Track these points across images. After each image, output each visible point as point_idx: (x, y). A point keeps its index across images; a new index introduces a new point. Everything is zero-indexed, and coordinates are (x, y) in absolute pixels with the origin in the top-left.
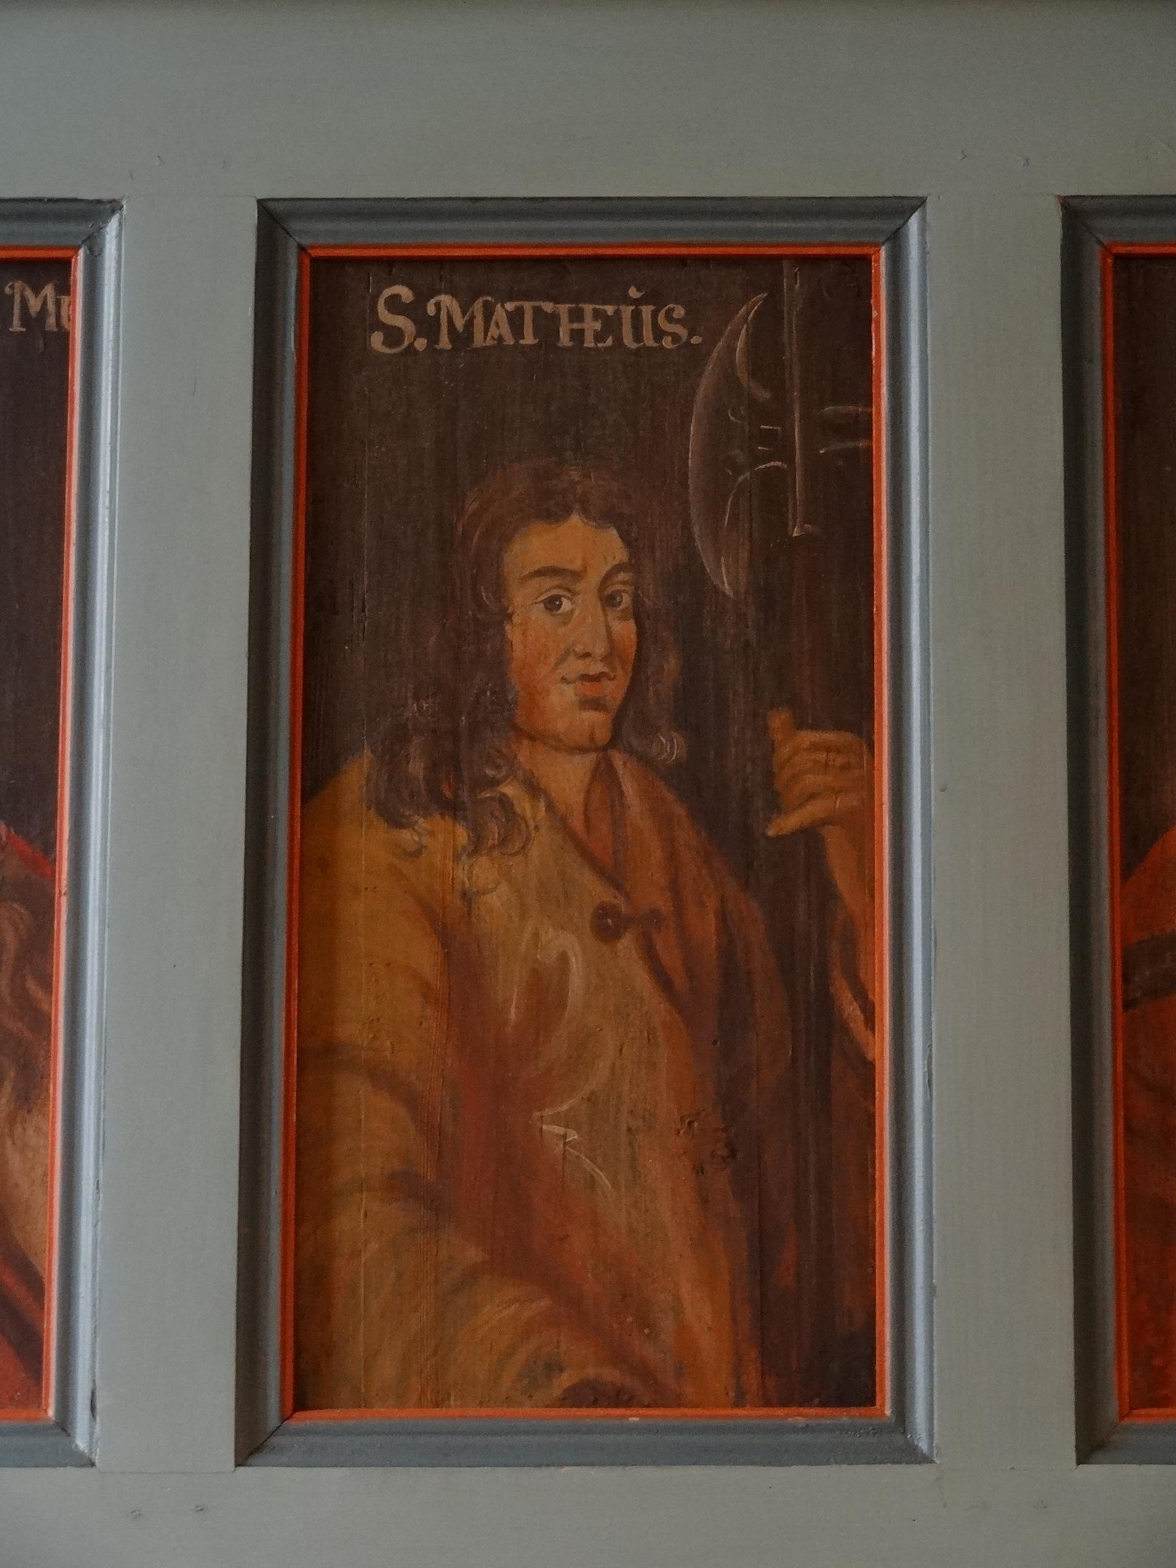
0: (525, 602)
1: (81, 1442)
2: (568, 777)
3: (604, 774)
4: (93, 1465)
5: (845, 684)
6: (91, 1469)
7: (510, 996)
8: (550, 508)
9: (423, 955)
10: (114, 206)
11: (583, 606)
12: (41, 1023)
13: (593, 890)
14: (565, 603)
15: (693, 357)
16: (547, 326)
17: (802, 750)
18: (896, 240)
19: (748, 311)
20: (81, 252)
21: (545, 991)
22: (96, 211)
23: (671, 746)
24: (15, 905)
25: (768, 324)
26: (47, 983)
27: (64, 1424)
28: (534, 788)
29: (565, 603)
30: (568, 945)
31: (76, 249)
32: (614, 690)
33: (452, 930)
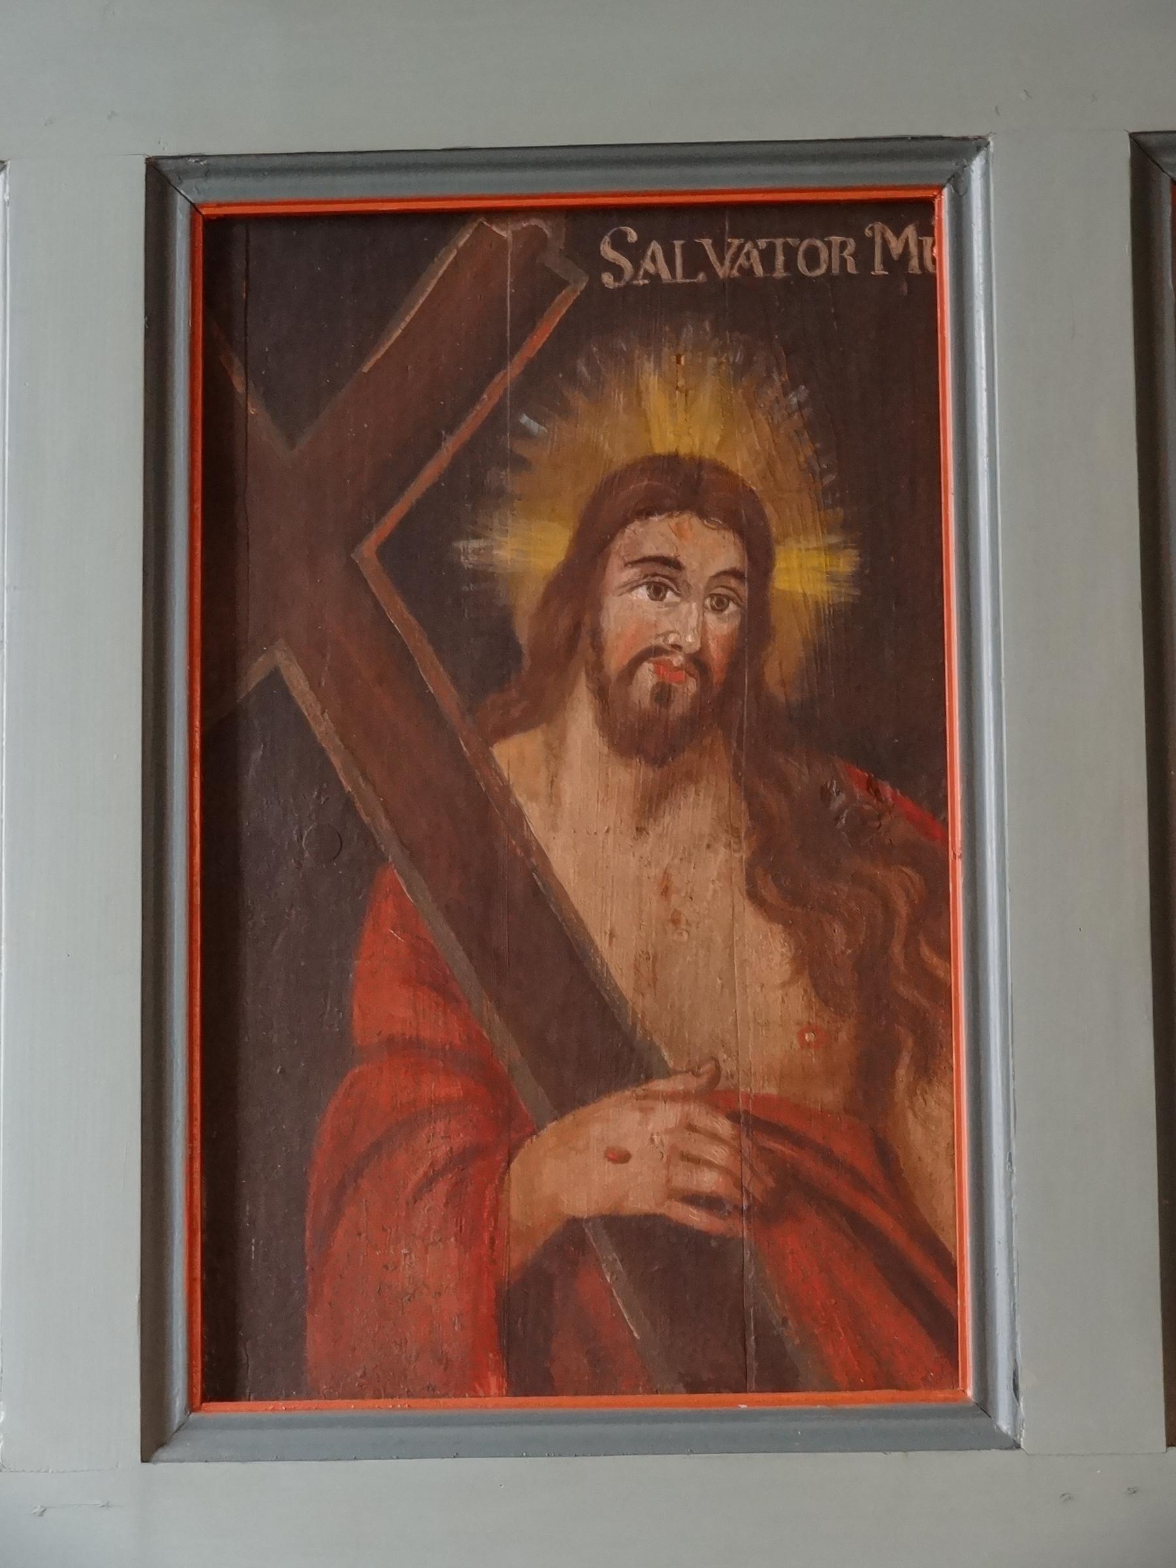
1: (1004, 1424)
4: (1018, 1447)
6: (1017, 1451)
10: (978, 144)
12: (941, 992)
20: (945, 191)
22: (964, 148)
24: (904, 869)
26: (945, 951)
27: (985, 1405)
31: (940, 188)
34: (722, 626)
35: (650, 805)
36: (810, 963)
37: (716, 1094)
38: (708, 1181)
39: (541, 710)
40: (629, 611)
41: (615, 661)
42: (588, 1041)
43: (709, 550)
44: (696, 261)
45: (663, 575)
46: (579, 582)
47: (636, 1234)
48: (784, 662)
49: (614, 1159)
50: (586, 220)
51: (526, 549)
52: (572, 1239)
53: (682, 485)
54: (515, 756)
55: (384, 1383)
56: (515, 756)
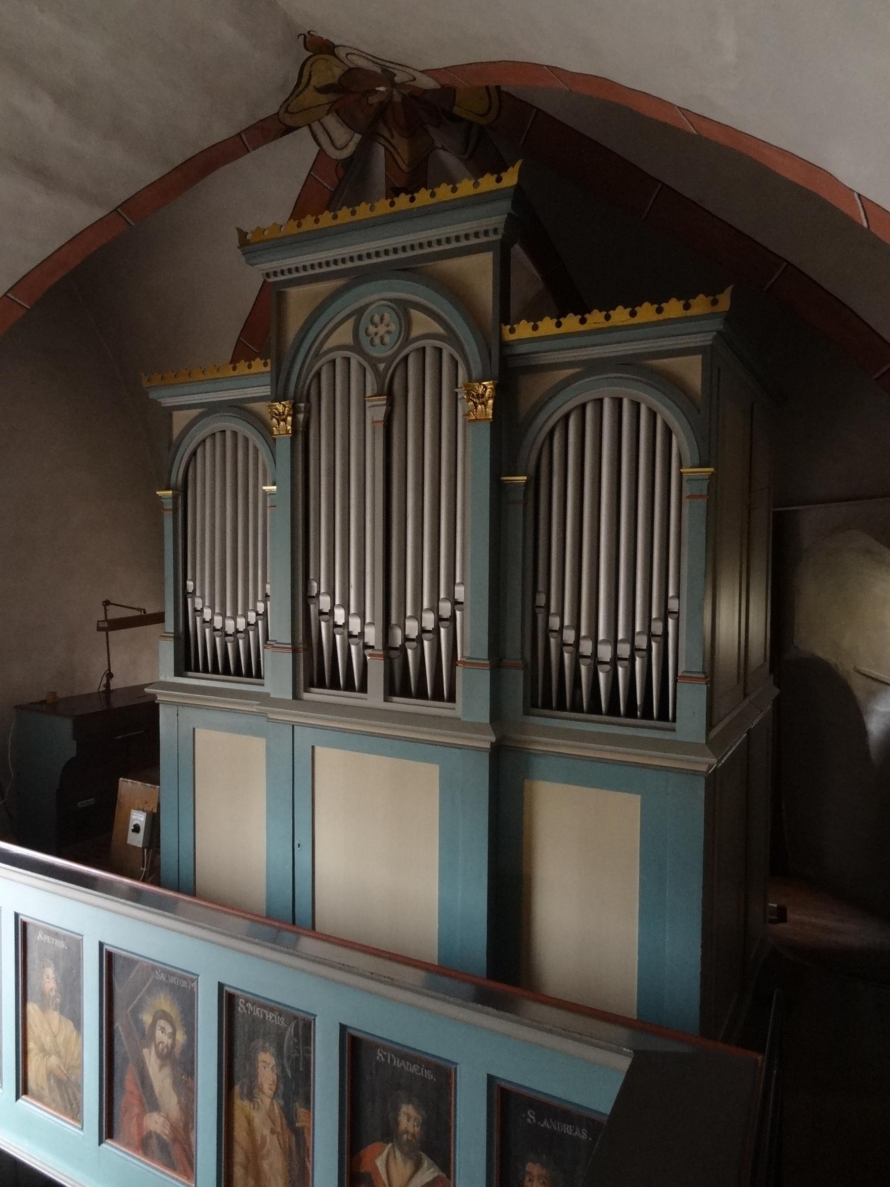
0: (261, 1065)
2: (267, 1101)
3: (272, 1104)
5: (308, 1101)
7: (258, 1138)
8: (264, 1050)
9: (246, 1124)
11: (269, 1070)
13: (269, 1123)
14: (267, 1069)
15: (286, 1029)
16: (264, 1016)
17: (301, 1111)
18: (314, 1019)
19: (293, 1025)
21: (264, 1138)
23: (282, 1103)
25: (296, 1027)
28: (262, 1101)
29: (267, 1069)
30: (266, 1132)
32: (274, 1087)
33: (250, 1122)
34: (170, 1041)
35: (161, 1067)
36: (179, 1102)
37: (167, 1117)
38: (167, 1132)
39: (148, 1046)
40: (158, 1033)
41: (158, 1041)
42: (151, 1103)
43: (169, 1030)
44: (167, 979)
45: (163, 1030)
46: (154, 1025)
47: (158, 1137)
48: (177, 1050)
49: (155, 1123)
50: (154, 968)
51: (147, 1018)
52: (150, 1135)
53: (164, 1015)
54: (145, 1051)
55: (128, 1145)
56: (145, 1051)
